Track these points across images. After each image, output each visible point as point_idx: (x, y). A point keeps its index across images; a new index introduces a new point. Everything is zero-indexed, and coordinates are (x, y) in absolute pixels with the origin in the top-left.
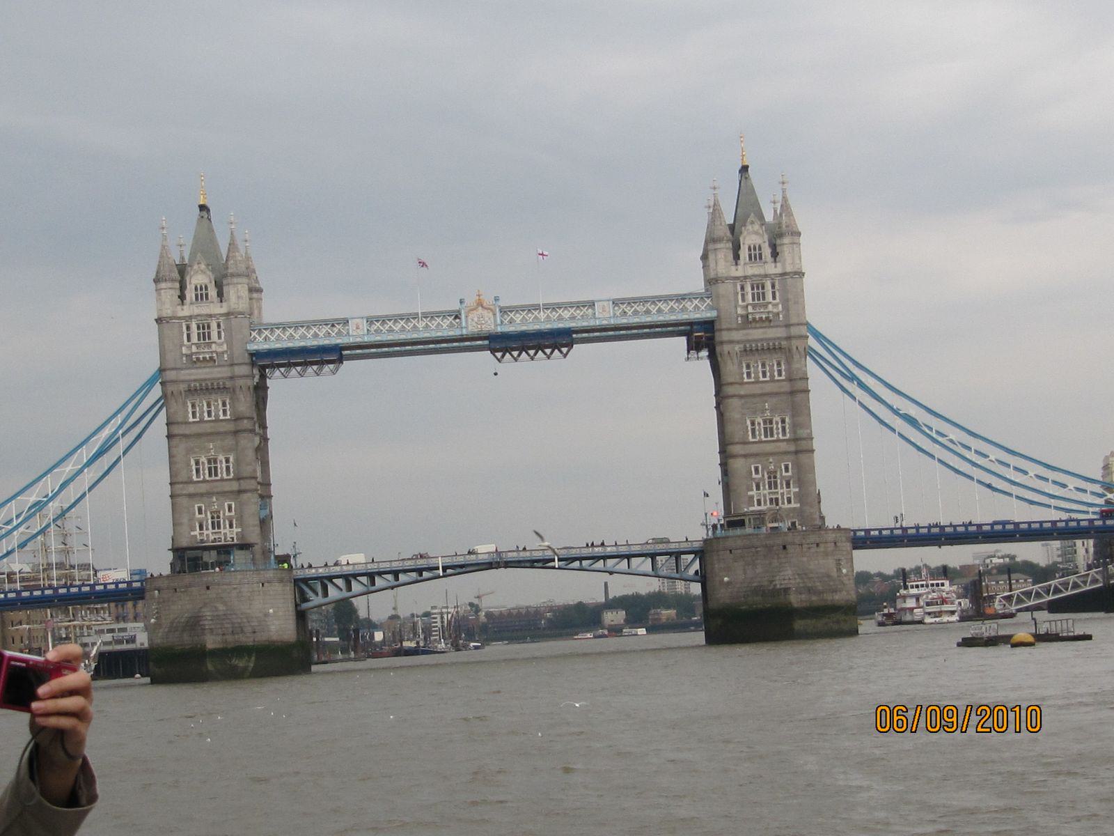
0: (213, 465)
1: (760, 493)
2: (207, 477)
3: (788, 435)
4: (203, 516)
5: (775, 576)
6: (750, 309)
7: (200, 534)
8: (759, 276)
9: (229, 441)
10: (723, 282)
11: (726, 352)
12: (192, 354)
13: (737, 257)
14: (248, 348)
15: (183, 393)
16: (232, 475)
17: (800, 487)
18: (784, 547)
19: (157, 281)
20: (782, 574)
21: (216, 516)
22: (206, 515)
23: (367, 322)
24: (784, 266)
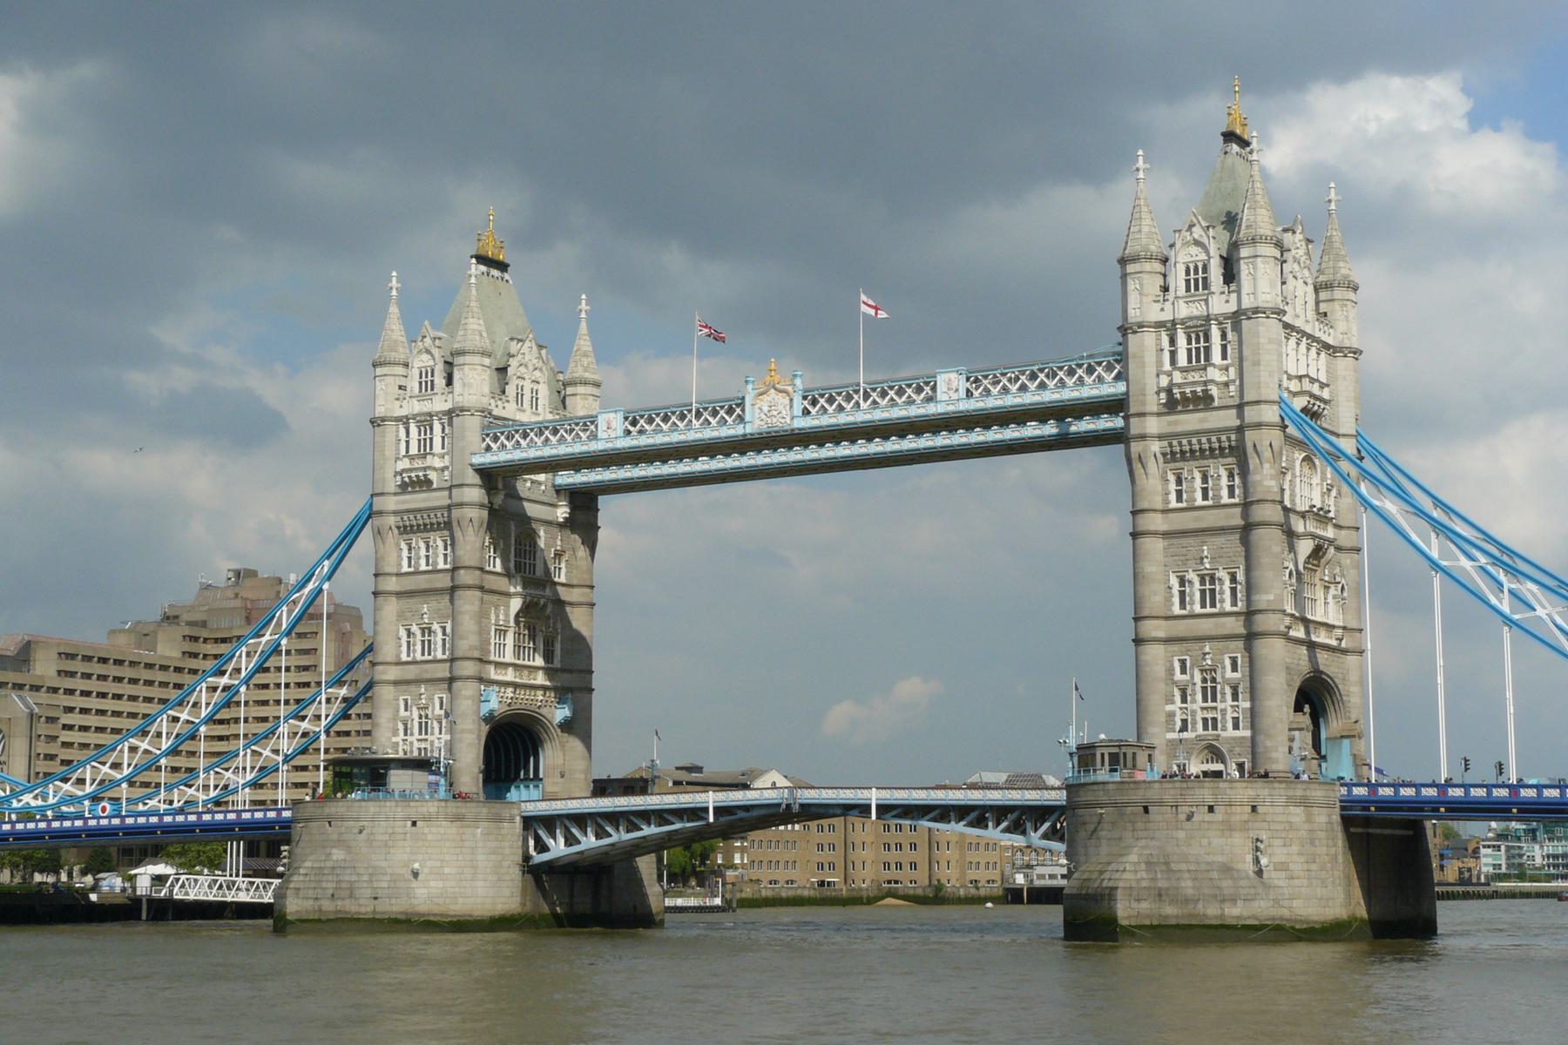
0: (427, 638)
1: (1186, 709)
2: (419, 657)
4: (408, 713)
5: (1109, 863)
8: (1197, 318)
10: (1135, 332)
11: (1133, 457)
13: (1165, 289)
15: (396, 531)
17: (1252, 699)
18: (1146, 810)
19: (374, 366)
20: (1120, 860)
22: (411, 711)
23: (626, 418)
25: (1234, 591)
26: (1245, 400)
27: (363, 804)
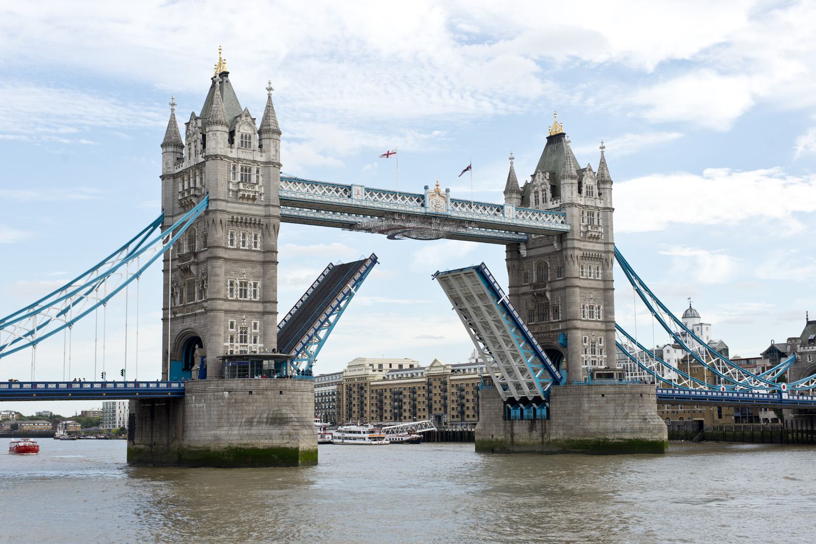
0: (243, 288)
2: (240, 299)
3: (602, 318)
4: (234, 330)
6: (590, 227)
7: (231, 345)
9: (259, 269)
10: (576, 207)
12: (239, 190)
13: (580, 191)
14: (280, 194)
16: (258, 298)
17: (607, 355)
18: (641, 394)
21: (244, 331)
22: (237, 329)
24: (605, 203)
25: (599, 312)
26: (611, 241)
27: (299, 382)
